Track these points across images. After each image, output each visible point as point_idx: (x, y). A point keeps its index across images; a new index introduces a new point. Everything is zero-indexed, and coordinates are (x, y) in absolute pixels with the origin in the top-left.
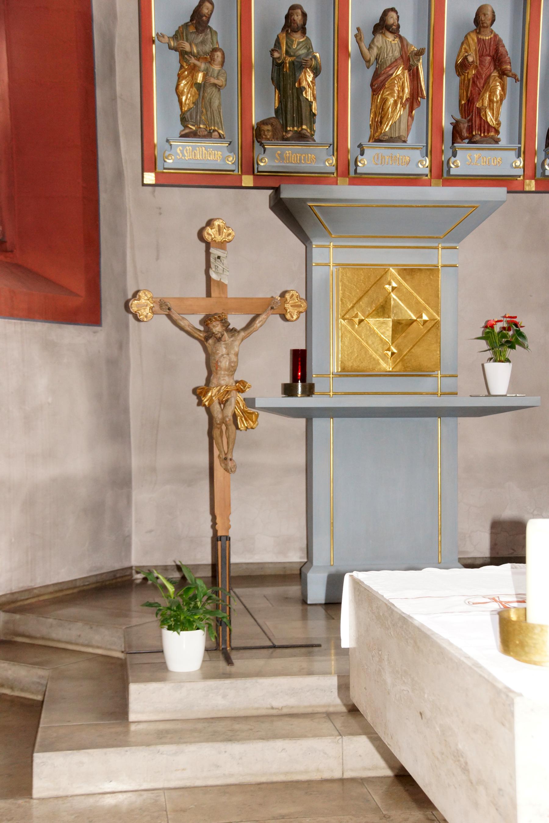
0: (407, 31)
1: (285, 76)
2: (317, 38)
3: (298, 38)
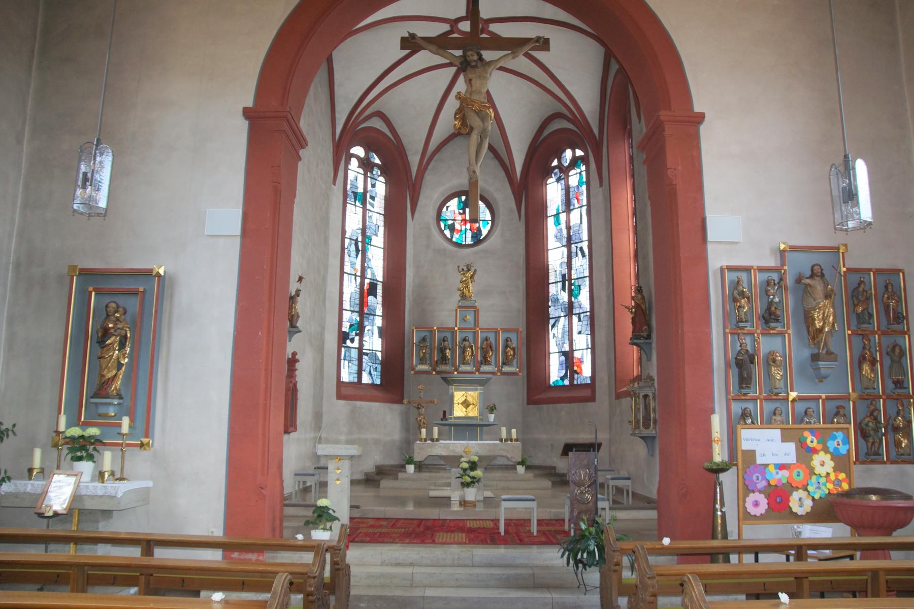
0: (471, 340)
1: (442, 351)
2: (448, 344)
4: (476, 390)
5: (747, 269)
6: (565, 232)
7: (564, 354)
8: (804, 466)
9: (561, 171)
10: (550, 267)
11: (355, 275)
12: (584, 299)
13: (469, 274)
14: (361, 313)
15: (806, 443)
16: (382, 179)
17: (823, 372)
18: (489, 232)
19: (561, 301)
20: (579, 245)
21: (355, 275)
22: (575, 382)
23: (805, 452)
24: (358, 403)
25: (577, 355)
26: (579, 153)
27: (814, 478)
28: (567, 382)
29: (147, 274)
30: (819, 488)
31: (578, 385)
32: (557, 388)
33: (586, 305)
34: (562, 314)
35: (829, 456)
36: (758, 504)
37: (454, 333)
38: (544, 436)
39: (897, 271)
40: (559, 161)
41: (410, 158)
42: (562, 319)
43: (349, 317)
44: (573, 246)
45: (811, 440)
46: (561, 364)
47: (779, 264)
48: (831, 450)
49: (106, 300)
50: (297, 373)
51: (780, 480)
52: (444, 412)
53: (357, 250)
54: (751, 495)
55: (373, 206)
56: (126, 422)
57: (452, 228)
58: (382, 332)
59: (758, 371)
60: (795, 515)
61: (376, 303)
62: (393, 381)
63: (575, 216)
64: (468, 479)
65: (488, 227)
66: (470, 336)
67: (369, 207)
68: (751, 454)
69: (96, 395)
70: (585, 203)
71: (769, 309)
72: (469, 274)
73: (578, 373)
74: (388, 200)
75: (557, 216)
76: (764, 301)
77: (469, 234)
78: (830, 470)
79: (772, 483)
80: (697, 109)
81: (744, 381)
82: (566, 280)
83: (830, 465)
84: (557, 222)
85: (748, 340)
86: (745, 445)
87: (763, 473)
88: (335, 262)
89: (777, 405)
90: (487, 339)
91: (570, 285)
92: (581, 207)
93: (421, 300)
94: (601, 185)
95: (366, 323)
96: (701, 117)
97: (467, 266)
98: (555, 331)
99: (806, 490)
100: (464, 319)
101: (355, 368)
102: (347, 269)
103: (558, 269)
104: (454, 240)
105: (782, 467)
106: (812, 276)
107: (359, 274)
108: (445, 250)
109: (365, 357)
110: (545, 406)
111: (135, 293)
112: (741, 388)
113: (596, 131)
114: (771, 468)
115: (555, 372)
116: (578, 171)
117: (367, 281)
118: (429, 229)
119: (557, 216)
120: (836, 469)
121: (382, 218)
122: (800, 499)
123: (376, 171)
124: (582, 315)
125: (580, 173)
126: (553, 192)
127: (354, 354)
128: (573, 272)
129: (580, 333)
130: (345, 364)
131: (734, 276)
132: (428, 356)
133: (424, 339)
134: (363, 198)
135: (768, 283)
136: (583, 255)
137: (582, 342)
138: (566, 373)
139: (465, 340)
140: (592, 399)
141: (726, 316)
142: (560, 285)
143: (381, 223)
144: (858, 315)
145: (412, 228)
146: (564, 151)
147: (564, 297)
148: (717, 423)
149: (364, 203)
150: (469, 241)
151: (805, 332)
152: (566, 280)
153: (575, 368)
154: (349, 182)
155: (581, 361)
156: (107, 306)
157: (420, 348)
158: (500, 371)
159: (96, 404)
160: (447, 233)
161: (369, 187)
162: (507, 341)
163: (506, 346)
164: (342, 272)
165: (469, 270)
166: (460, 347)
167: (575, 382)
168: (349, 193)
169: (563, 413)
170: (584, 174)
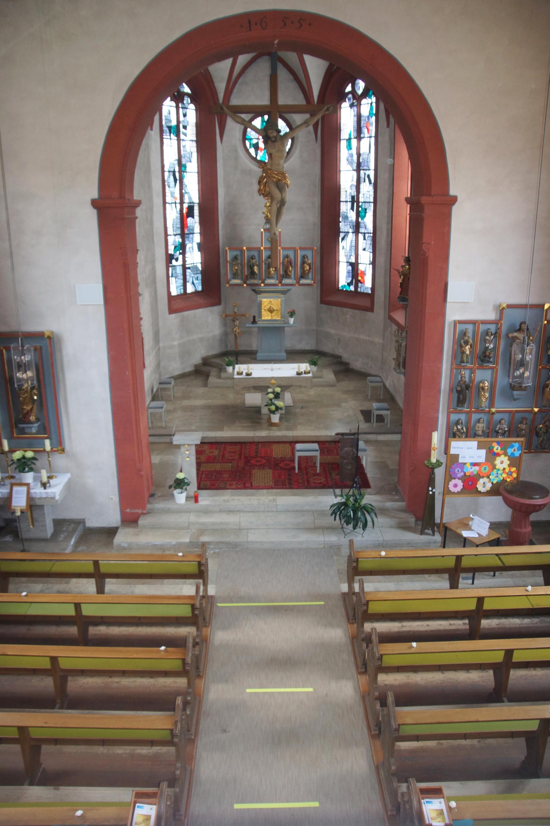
1: (251, 267)
3: (254, 261)
4: (279, 298)
5: (474, 322)
7: (351, 264)
8: (490, 464)
9: (354, 98)
10: (342, 187)
11: (175, 203)
12: (368, 221)
14: (183, 235)
15: (493, 450)
16: (192, 107)
17: (515, 397)
19: (350, 219)
20: (367, 172)
21: (175, 203)
23: (492, 455)
24: (186, 313)
25: (361, 267)
27: (495, 471)
28: (352, 288)
29: (40, 335)
30: (497, 477)
31: (360, 293)
33: (370, 228)
34: (351, 231)
35: (507, 458)
37: (260, 251)
38: (333, 331)
41: (216, 85)
43: (174, 240)
44: (362, 172)
45: (497, 448)
46: (348, 272)
47: (498, 318)
48: (509, 454)
50: (142, 327)
51: (472, 472)
52: (254, 317)
53: (175, 180)
54: (453, 480)
55: (185, 135)
56: (47, 442)
57: (256, 147)
58: (201, 247)
60: (480, 492)
61: (194, 223)
62: (212, 286)
63: (365, 143)
64: (273, 408)
67: (182, 137)
68: (457, 456)
70: (373, 135)
71: (484, 352)
73: (361, 283)
74: (199, 126)
75: (349, 140)
76: (482, 345)
79: (467, 474)
81: (461, 402)
82: (355, 200)
83: (507, 462)
84: (349, 147)
85: (466, 373)
86: (453, 451)
87: (462, 468)
88: (158, 201)
89: (481, 415)
90: (287, 256)
91: (358, 207)
92: (370, 137)
93: (231, 216)
94: (388, 126)
95: (187, 242)
96: (454, 199)
98: (344, 242)
99: (488, 477)
101: (181, 282)
102: (169, 199)
104: (259, 158)
105: (475, 464)
106: (520, 330)
107: (178, 201)
108: (250, 170)
109: (188, 271)
110: (334, 307)
112: (458, 406)
114: (468, 465)
115: (343, 279)
117: (185, 206)
118: (236, 151)
119: (349, 140)
120: (509, 466)
121: (194, 144)
122: (484, 483)
123: (187, 100)
124: (367, 235)
125: (371, 104)
126: (347, 115)
127: (179, 270)
128: (361, 196)
129: (364, 249)
130: (172, 280)
131: (464, 327)
132: (239, 272)
133: (236, 258)
134: (176, 131)
135: (487, 333)
136: (370, 183)
137: (365, 258)
138: (352, 280)
140: (371, 309)
141: (454, 356)
142: (349, 204)
143: (194, 150)
145: (221, 150)
147: (352, 216)
148: (436, 438)
149: (178, 135)
152: (355, 200)
153: (360, 278)
154: (164, 118)
155: (363, 273)
157: (232, 266)
158: (298, 282)
160: (252, 151)
161: (182, 118)
162: (304, 257)
163: (303, 263)
164: (165, 203)
166: (265, 263)
167: (359, 290)
168: (165, 128)
169: (348, 316)
170: (374, 105)
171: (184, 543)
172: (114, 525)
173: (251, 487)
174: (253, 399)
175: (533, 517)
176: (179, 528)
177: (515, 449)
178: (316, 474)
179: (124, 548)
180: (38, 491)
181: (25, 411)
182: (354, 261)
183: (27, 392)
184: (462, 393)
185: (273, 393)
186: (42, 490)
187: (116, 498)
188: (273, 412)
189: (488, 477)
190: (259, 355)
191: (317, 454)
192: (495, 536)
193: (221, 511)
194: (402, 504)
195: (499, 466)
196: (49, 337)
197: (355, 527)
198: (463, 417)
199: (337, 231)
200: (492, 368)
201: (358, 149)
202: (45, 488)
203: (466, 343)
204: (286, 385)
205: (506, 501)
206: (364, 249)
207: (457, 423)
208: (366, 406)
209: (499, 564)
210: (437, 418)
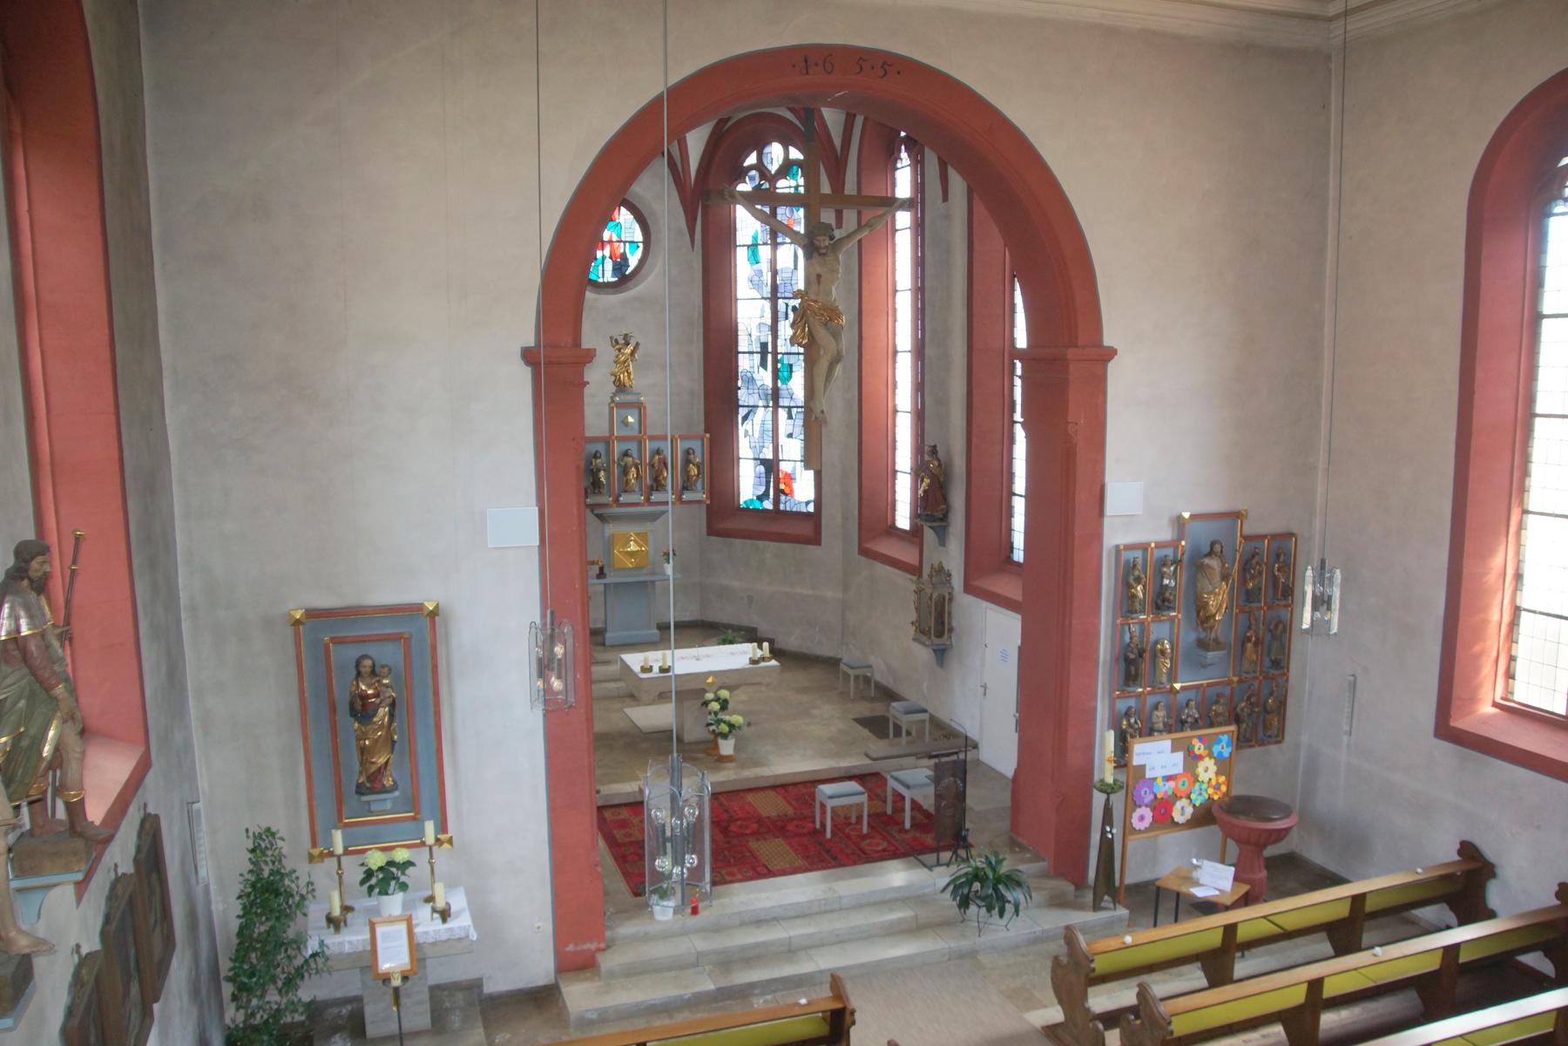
0: (635, 453)
1: (594, 474)
5: (1144, 547)
6: (767, 277)
10: (740, 327)
12: (796, 385)
13: (628, 351)
18: (642, 262)
19: (759, 383)
22: (782, 507)
23: (1192, 759)
25: (785, 467)
26: (795, 154)
28: (768, 505)
31: (785, 512)
32: (748, 512)
36: (1142, 817)
38: (736, 584)
39: (1291, 535)
40: (760, 157)
42: (760, 411)
45: (1198, 747)
49: (353, 652)
59: (1145, 666)
60: (1177, 824)
64: (724, 728)
65: (639, 253)
66: (633, 447)
68: (1142, 768)
69: (361, 790)
72: (628, 351)
75: (753, 247)
76: (1153, 583)
77: (609, 265)
78: (1213, 776)
80: (1108, 340)
83: (1213, 768)
84: (754, 258)
87: (1151, 787)
90: (658, 452)
91: (775, 361)
96: (1112, 353)
97: (626, 337)
98: (748, 422)
99: (1189, 797)
100: (625, 423)
103: (755, 334)
105: (1169, 778)
106: (1210, 554)
110: (738, 542)
111: (396, 638)
113: (837, 142)
114: (1160, 782)
115: (748, 486)
116: (793, 183)
119: (753, 247)
120: (1218, 774)
124: (794, 411)
129: (790, 436)
137: (792, 450)
139: (626, 454)
140: (815, 540)
142: (757, 357)
144: (1248, 592)
146: (769, 143)
147: (765, 378)
150: (609, 277)
151: (1194, 615)
153: (782, 486)
155: (790, 478)
156: (358, 663)
159: (368, 803)
162: (688, 452)
163: (687, 462)
165: (627, 344)
167: (782, 507)
171: (707, 993)
172: (541, 982)
173: (770, 874)
174: (660, 716)
175: (1270, 851)
176: (680, 966)
177: (1224, 748)
178: (864, 837)
179: (591, 1023)
180: (428, 926)
181: (373, 768)
182: (770, 456)
183: (381, 727)
184: (1133, 664)
185: (717, 699)
186: (437, 924)
187: (547, 926)
188: (725, 736)
189: (1189, 797)
190: (610, 636)
191: (864, 798)
192: (1245, 888)
193: (743, 924)
194: (1043, 865)
195: (1203, 777)
196: (433, 614)
197: (1001, 915)
198: (1132, 702)
199: (734, 405)
200: (1172, 619)
201: (773, 262)
202: (444, 920)
203: (1138, 580)
204: (731, 680)
205: (1228, 832)
206: (790, 436)
207: (1127, 715)
208: (865, 709)
209: (1277, 930)
210: (1095, 709)
